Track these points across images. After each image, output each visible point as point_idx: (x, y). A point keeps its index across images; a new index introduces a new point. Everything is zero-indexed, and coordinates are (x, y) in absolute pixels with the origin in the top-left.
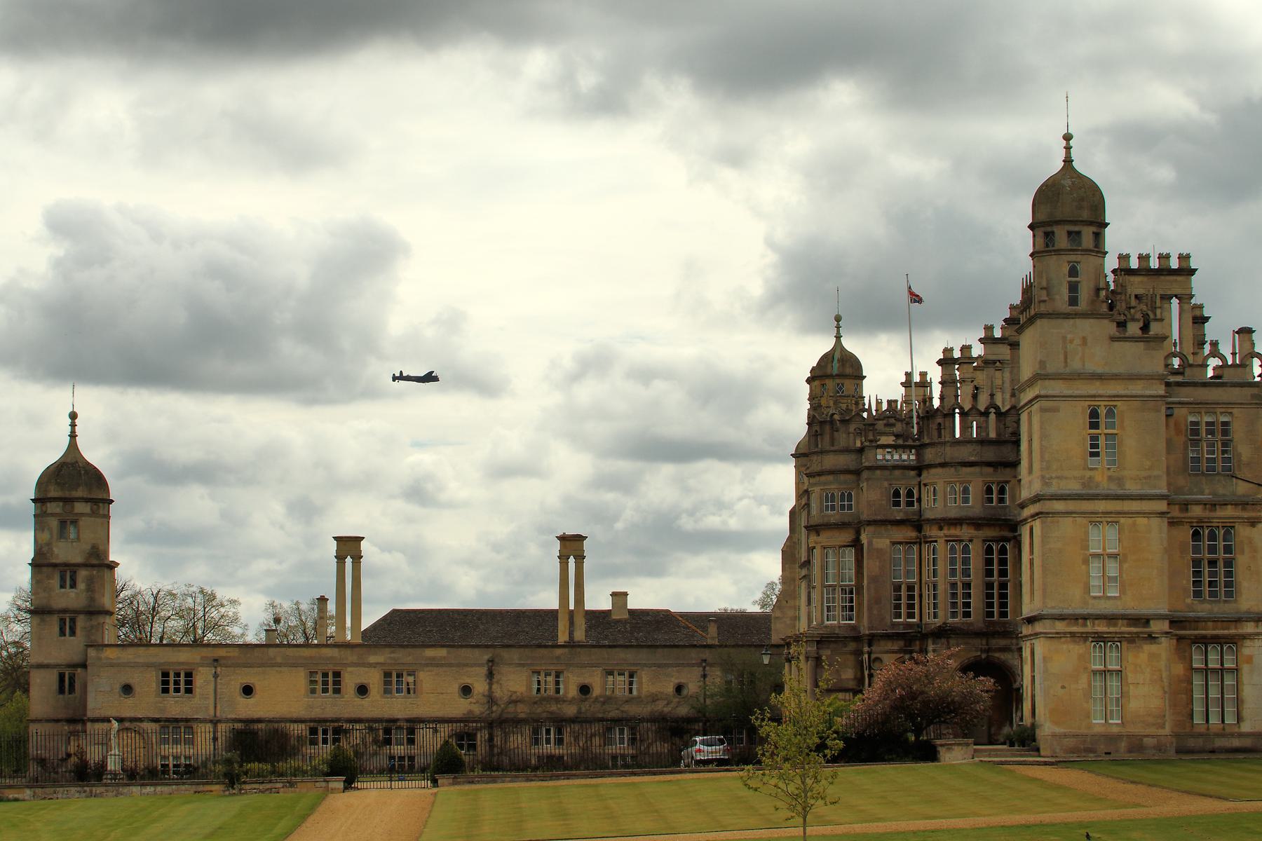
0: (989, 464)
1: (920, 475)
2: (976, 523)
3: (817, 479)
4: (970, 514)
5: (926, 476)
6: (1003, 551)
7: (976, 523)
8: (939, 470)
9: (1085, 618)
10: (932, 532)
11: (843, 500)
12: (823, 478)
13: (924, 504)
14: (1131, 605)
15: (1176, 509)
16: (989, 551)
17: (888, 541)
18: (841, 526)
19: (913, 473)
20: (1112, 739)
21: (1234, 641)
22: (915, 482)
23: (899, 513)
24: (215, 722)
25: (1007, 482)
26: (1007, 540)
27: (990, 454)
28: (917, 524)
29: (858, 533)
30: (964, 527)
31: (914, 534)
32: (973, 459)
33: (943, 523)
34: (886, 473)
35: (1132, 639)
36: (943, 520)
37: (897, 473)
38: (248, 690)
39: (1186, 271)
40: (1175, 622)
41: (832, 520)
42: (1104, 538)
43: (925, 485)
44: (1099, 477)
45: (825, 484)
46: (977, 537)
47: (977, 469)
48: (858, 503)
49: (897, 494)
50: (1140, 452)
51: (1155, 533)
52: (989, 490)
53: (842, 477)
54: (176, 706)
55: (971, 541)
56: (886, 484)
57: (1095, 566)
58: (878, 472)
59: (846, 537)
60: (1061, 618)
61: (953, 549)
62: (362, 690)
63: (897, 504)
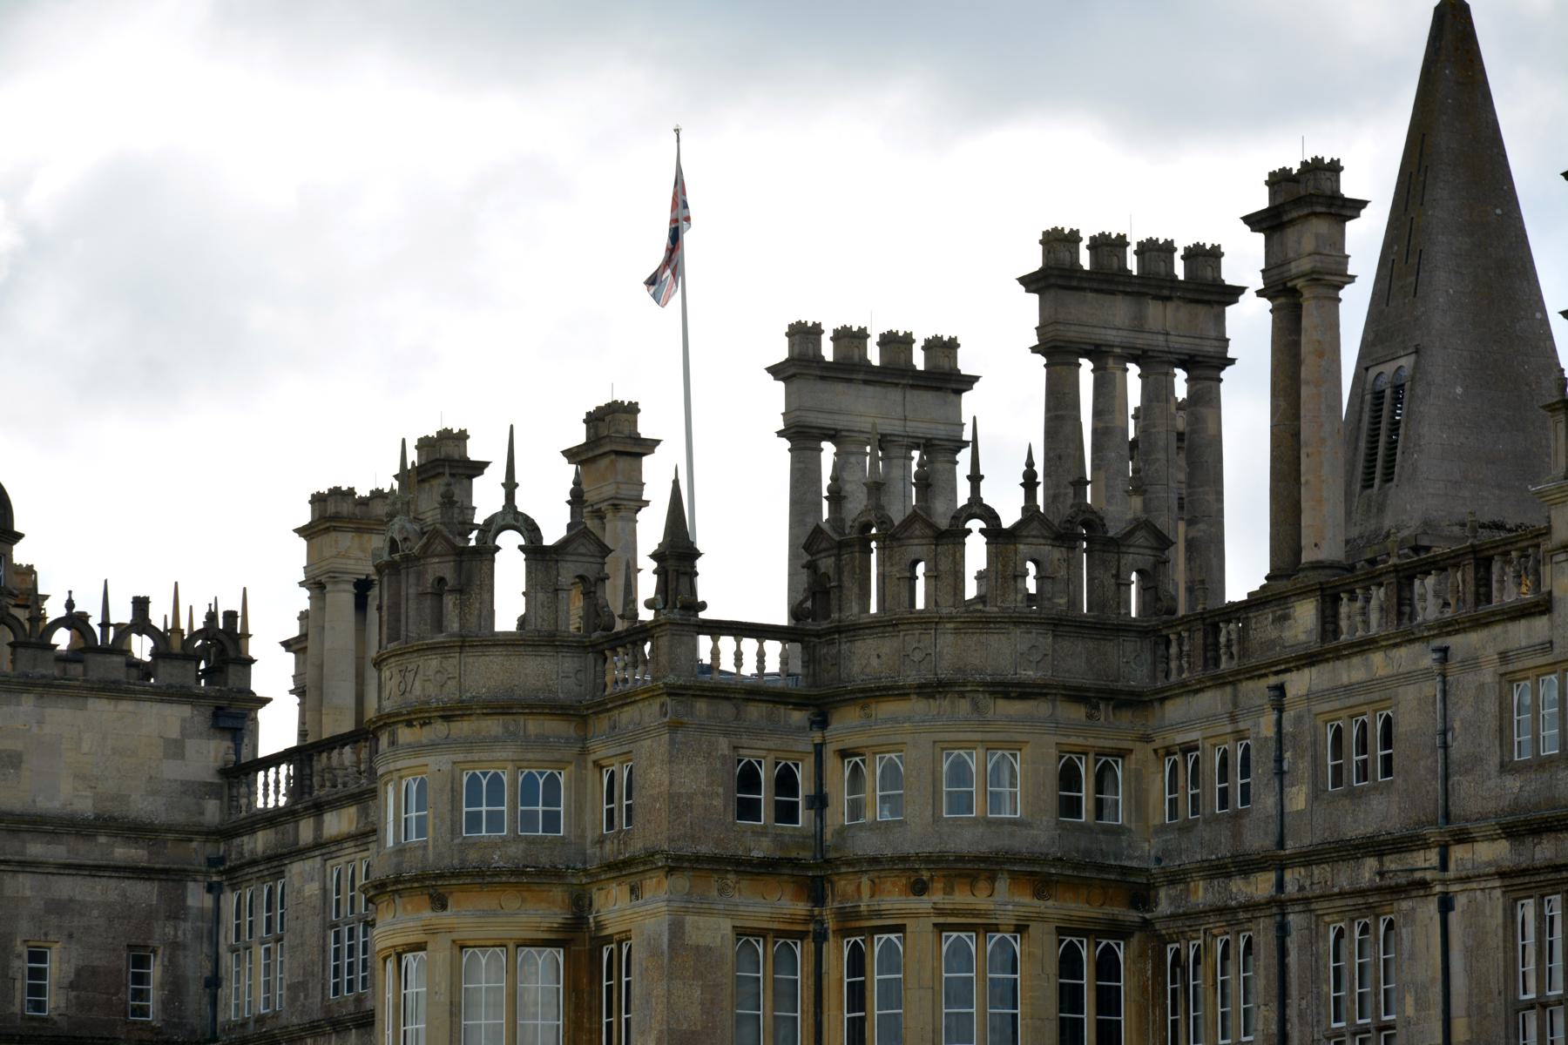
0: (1076, 695)
1: (822, 722)
2: (1039, 875)
3: (440, 729)
4: (1019, 843)
5: (847, 726)
6: (1107, 966)
7: (1039, 875)
8: (916, 706)
10: (894, 900)
11: (529, 796)
12: (463, 728)
13: (838, 814)
16: (1069, 963)
17: (726, 926)
18: (525, 877)
19: (798, 717)
22: (805, 744)
23: (760, 838)
25: (1122, 754)
26: (1119, 931)
27: (1077, 661)
28: (813, 873)
29: (580, 905)
30: (1002, 885)
31: (801, 908)
32: (1030, 674)
33: (920, 871)
34: (727, 709)
36: (937, 861)
37: (755, 711)
41: (497, 859)
43: (844, 754)
45: (470, 743)
46: (1041, 918)
47: (1040, 708)
48: (578, 809)
49: (749, 779)
52: (1069, 777)
53: (533, 726)
55: (1021, 929)
56: (723, 745)
58: (702, 706)
59: (546, 912)
61: (960, 956)
63: (748, 810)
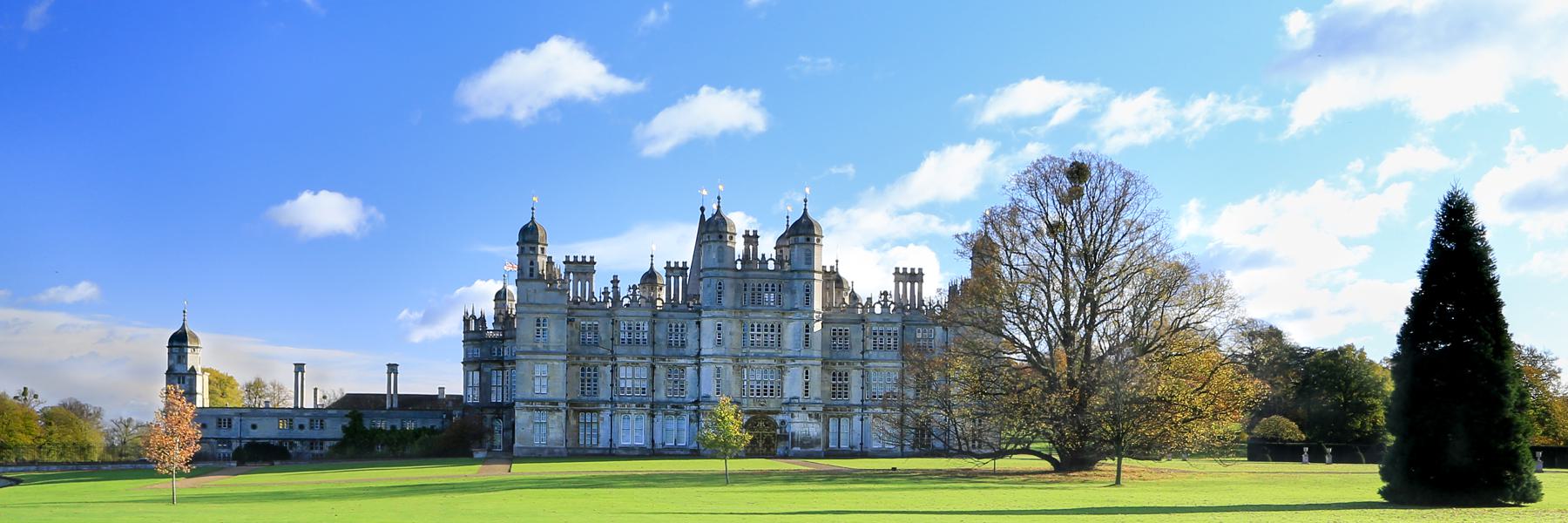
9: (532, 401)
14: (551, 396)
15: (572, 356)
20: (541, 449)
21: (598, 411)
24: (240, 439)
35: (551, 410)
38: (254, 427)
39: (593, 263)
40: (571, 403)
42: (540, 369)
44: (540, 346)
50: (556, 334)
51: (560, 368)
54: (224, 433)
57: (537, 382)
60: (522, 401)
62: (301, 427)
